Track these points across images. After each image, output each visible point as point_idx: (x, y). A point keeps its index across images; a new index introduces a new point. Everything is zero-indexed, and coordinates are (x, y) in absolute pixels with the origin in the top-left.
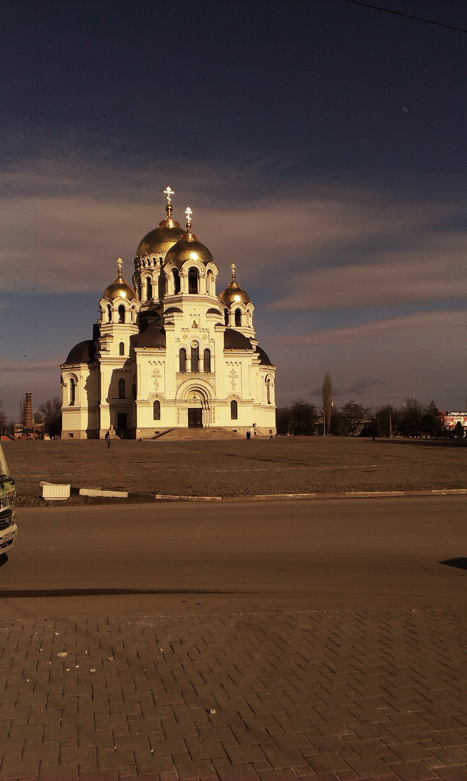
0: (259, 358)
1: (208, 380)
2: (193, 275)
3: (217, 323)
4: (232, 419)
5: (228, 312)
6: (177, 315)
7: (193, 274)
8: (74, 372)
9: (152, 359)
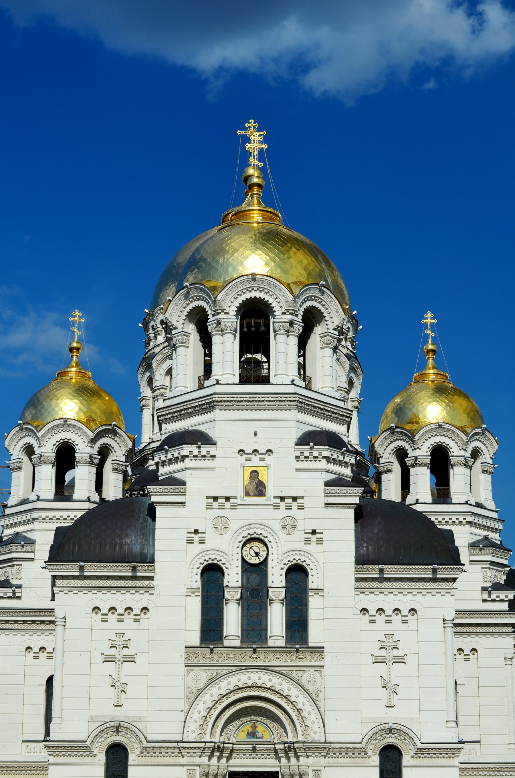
1: (300, 673)
2: (258, 325)
3: (333, 476)
5: (407, 457)
6: (195, 452)
7: (255, 323)
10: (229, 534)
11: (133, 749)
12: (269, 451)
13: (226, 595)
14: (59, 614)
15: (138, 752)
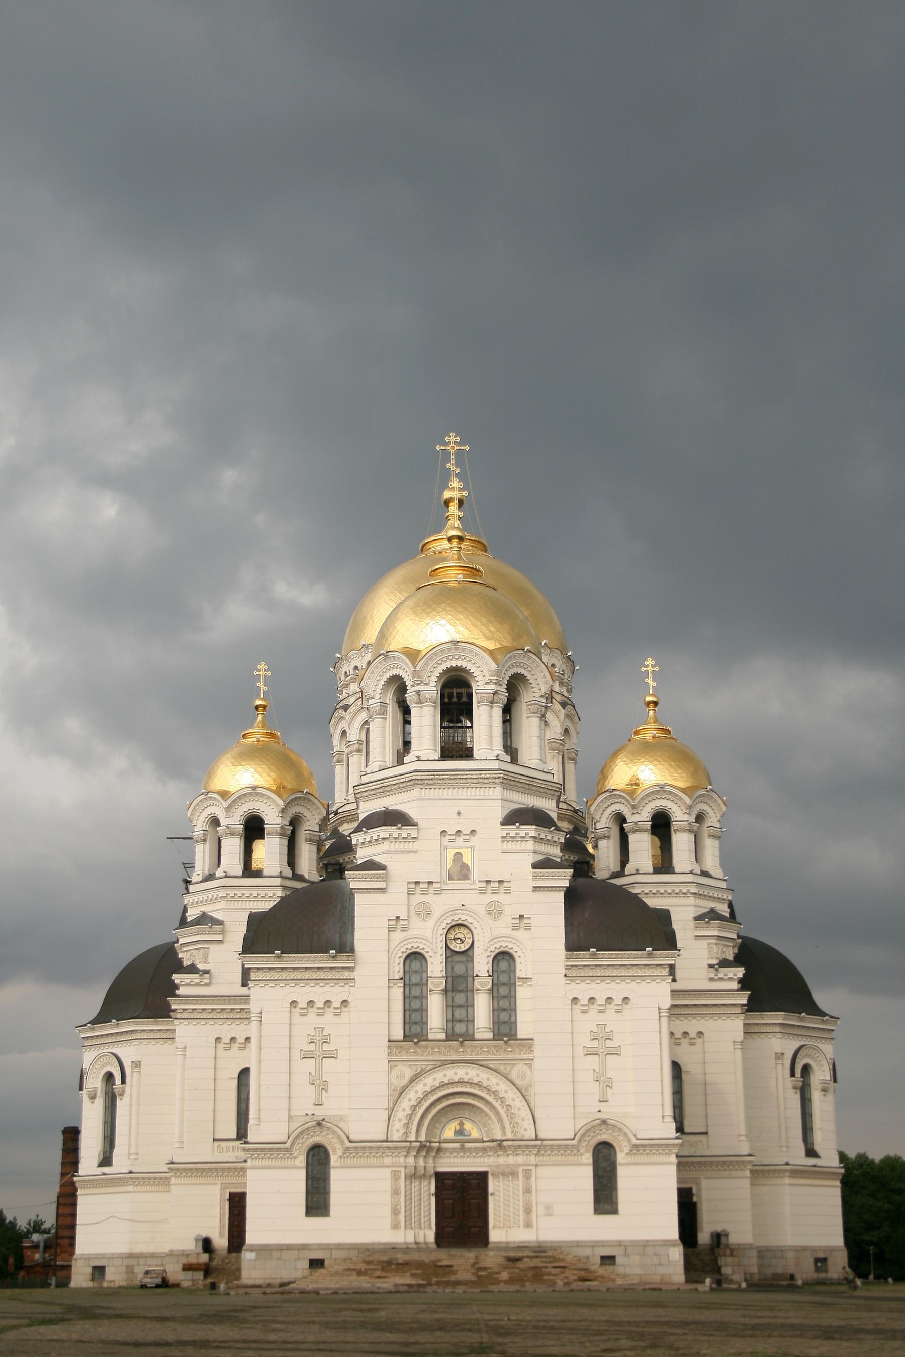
0: (744, 983)
2: (459, 695)
3: (541, 858)
4: (598, 1210)
7: (457, 693)
8: (114, 1051)
9: (303, 993)
10: (431, 922)
11: (334, 1150)
12: (473, 831)
13: (430, 986)
14: (254, 1006)
15: (340, 1153)
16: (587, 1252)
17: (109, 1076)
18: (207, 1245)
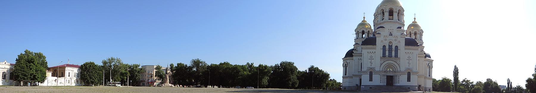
9: (369, 51)
16: (406, 87)
17: (346, 64)
18: (357, 85)
